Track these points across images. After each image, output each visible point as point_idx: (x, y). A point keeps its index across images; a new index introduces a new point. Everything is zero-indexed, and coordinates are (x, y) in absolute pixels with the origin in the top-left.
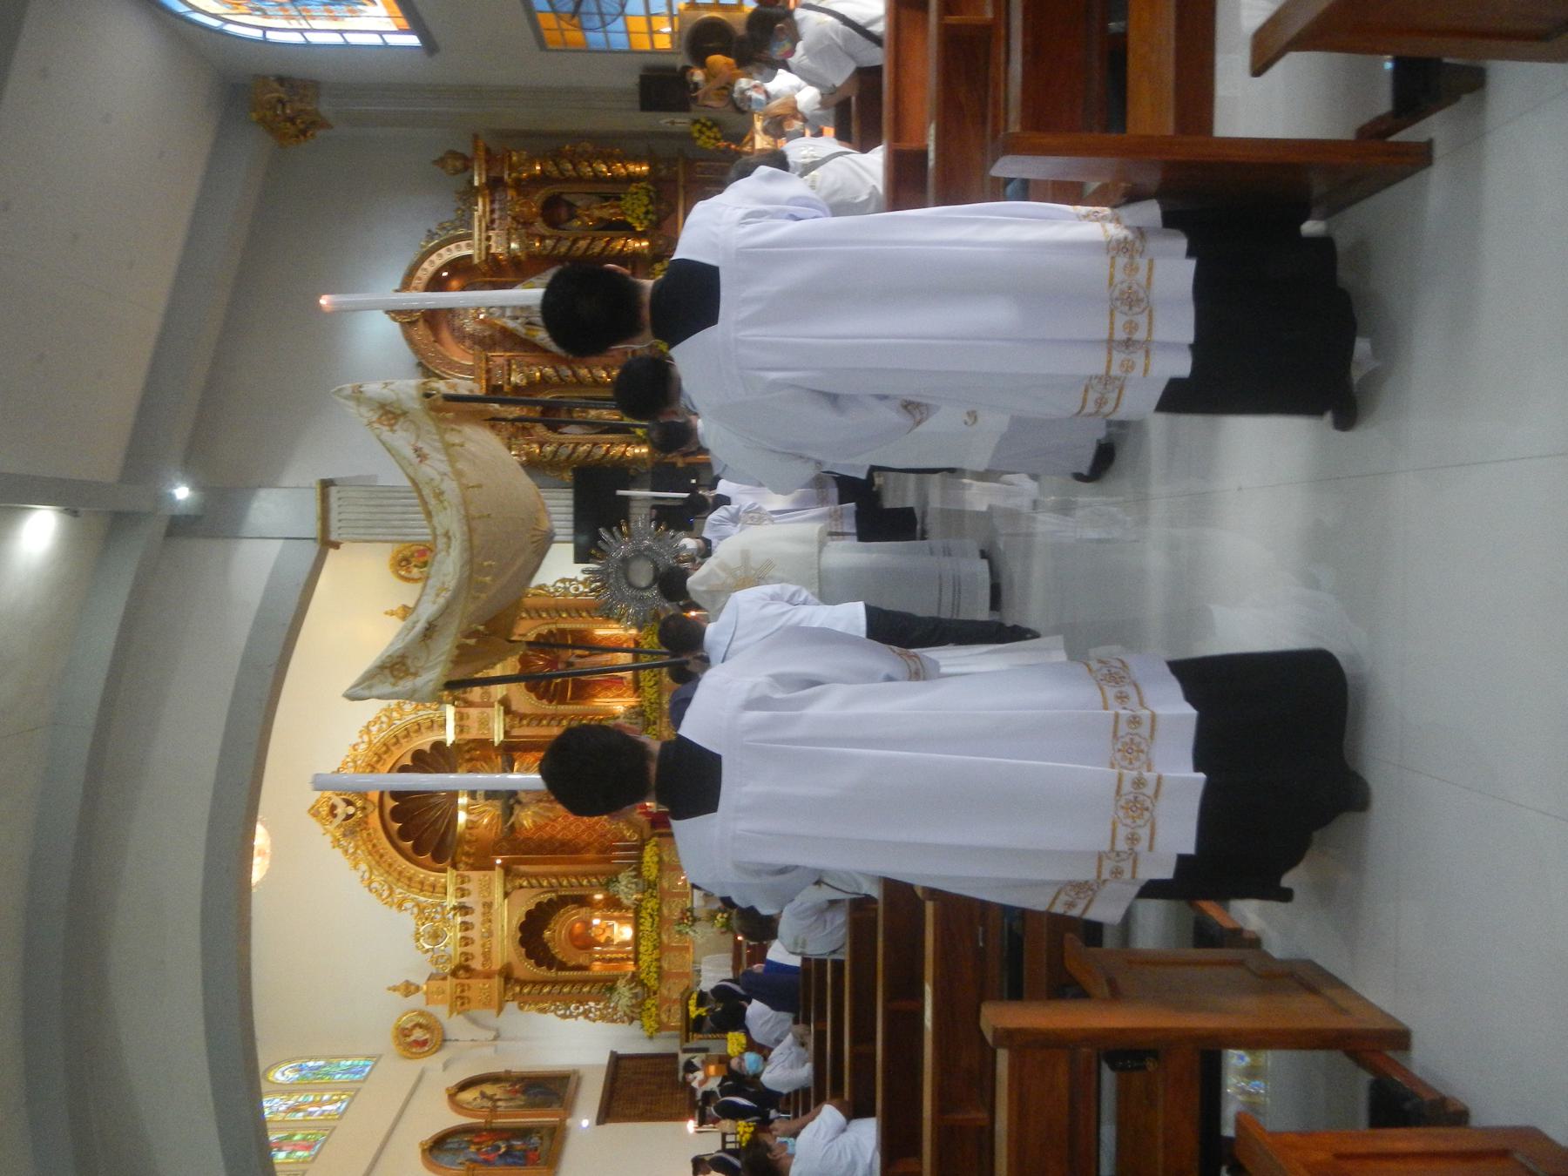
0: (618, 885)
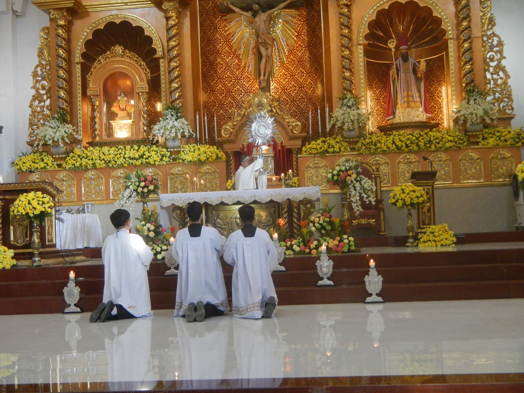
0: (174, 118)
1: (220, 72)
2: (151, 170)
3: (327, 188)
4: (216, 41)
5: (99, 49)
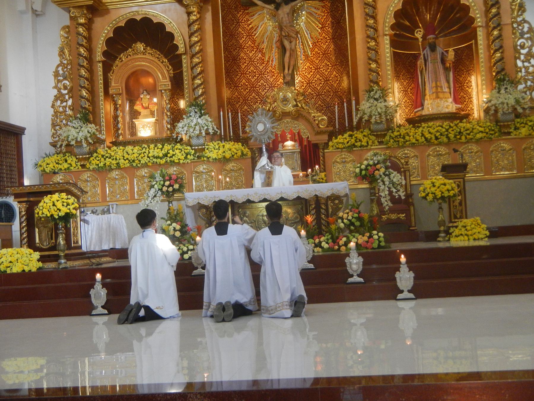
0: (198, 115)
1: (243, 67)
2: (175, 169)
3: (356, 183)
4: (238, 35)
5: (120, 47)
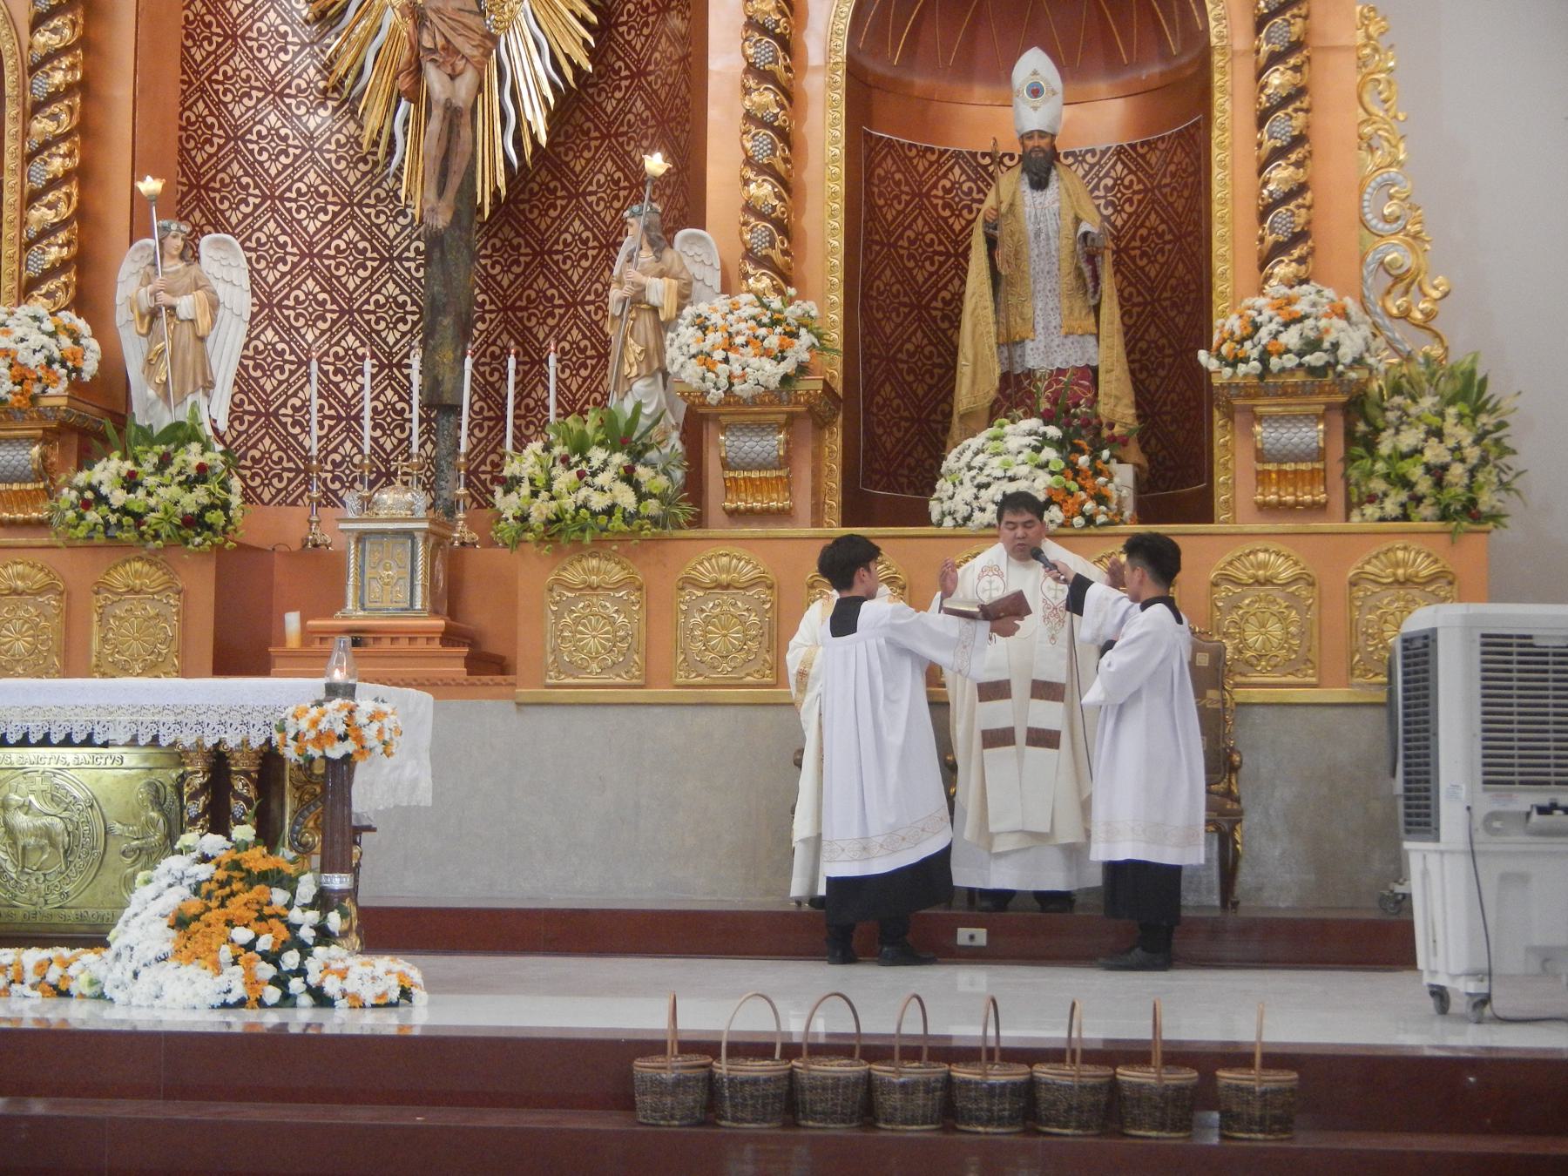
1: (273, 172)
4: (263, 40)
